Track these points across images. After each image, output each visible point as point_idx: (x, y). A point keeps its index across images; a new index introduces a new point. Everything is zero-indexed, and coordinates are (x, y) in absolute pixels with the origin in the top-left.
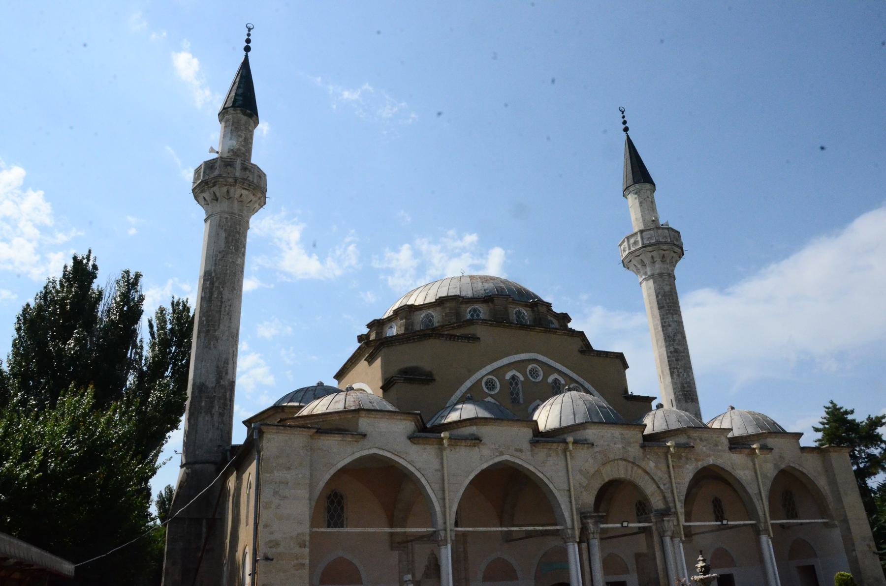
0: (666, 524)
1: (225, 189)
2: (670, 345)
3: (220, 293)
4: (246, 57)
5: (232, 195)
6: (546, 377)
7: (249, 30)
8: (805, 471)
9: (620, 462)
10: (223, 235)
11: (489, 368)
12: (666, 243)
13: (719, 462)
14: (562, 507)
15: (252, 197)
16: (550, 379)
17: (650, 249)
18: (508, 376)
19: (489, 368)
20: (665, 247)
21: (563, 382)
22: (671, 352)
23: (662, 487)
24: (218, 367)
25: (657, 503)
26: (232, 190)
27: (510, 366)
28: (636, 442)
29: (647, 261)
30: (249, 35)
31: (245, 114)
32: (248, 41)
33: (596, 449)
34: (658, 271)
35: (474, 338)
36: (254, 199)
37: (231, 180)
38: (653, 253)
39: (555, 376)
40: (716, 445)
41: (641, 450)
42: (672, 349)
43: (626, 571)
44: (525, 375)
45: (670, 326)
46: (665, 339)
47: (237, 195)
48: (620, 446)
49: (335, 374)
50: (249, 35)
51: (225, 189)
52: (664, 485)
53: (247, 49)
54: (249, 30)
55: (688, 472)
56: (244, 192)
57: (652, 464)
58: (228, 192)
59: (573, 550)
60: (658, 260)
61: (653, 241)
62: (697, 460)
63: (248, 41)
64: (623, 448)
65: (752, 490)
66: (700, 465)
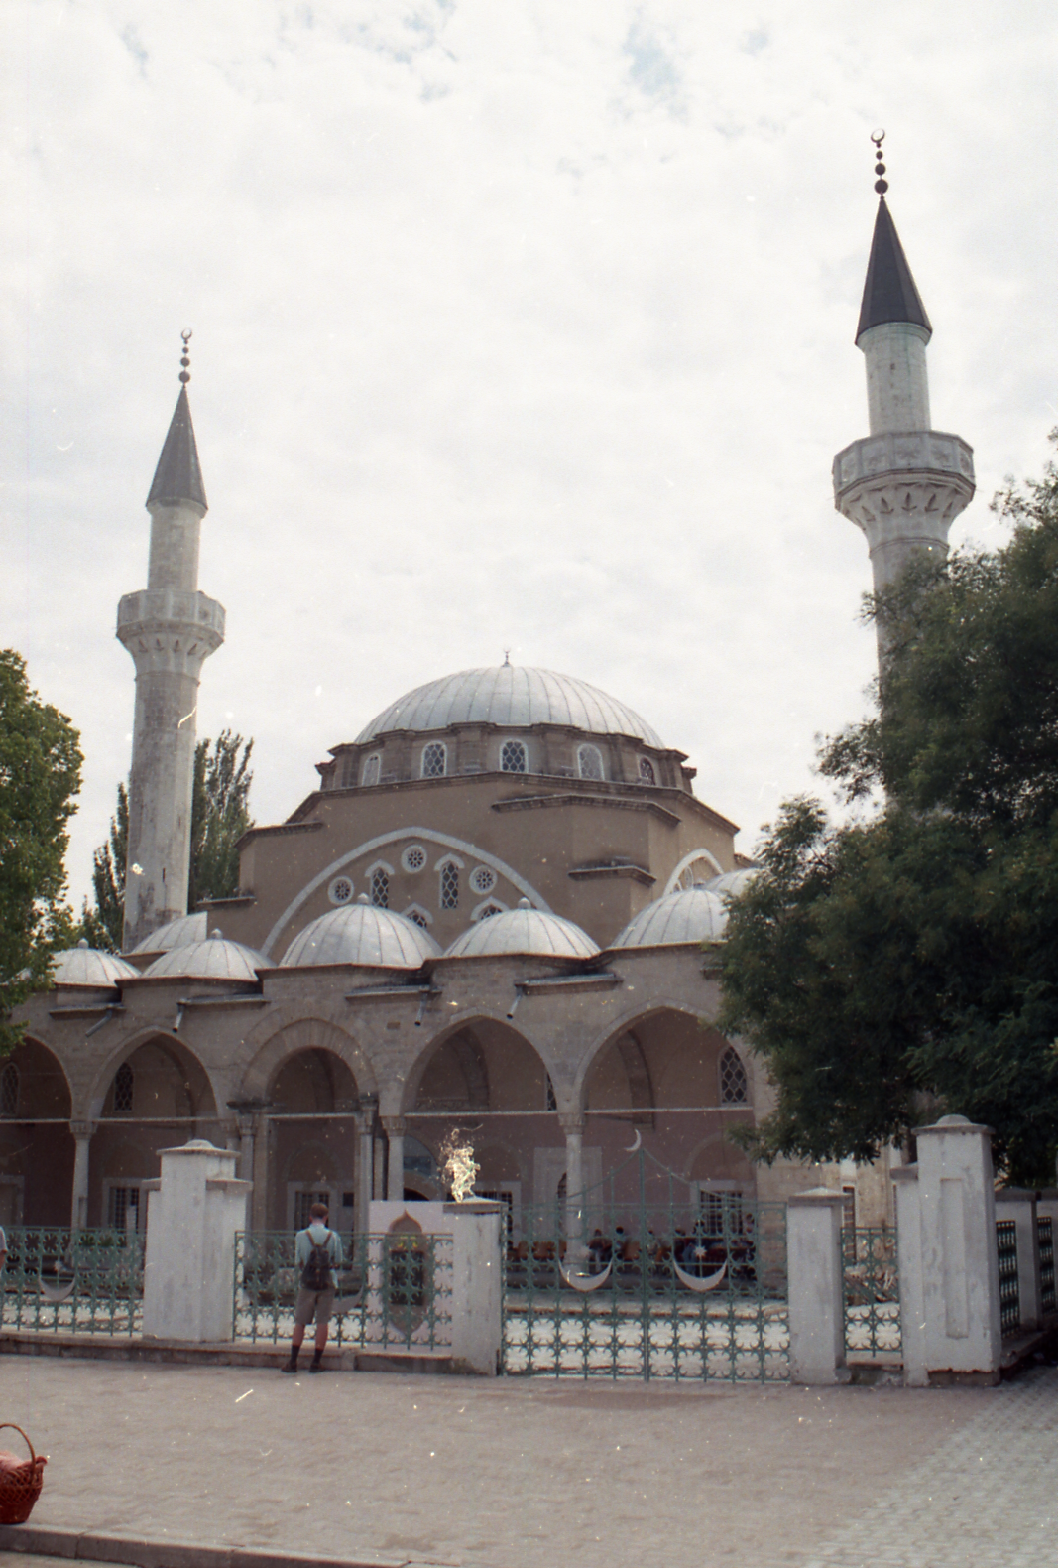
3: (140, 794)
6: (431, 864)
10: (143, 706)
11: (336, 866)
12: (874, 477)
15: (174, 638)
16: (439, 867)
18: (369, 873)
19: (336, 866)
21: (460, 864)
24: (140, 896)
25: (364, 1086)
26: (144, 642)
30: (186, 351)
32: (185, 362)
33: (274, 1007)
35: (318, 826)
50: (186, 351)
51: (135, 640)
53: (184, 377)
56: (161, 637)
58: (140, 643)
61: (853, 478)
63: (185, 362)
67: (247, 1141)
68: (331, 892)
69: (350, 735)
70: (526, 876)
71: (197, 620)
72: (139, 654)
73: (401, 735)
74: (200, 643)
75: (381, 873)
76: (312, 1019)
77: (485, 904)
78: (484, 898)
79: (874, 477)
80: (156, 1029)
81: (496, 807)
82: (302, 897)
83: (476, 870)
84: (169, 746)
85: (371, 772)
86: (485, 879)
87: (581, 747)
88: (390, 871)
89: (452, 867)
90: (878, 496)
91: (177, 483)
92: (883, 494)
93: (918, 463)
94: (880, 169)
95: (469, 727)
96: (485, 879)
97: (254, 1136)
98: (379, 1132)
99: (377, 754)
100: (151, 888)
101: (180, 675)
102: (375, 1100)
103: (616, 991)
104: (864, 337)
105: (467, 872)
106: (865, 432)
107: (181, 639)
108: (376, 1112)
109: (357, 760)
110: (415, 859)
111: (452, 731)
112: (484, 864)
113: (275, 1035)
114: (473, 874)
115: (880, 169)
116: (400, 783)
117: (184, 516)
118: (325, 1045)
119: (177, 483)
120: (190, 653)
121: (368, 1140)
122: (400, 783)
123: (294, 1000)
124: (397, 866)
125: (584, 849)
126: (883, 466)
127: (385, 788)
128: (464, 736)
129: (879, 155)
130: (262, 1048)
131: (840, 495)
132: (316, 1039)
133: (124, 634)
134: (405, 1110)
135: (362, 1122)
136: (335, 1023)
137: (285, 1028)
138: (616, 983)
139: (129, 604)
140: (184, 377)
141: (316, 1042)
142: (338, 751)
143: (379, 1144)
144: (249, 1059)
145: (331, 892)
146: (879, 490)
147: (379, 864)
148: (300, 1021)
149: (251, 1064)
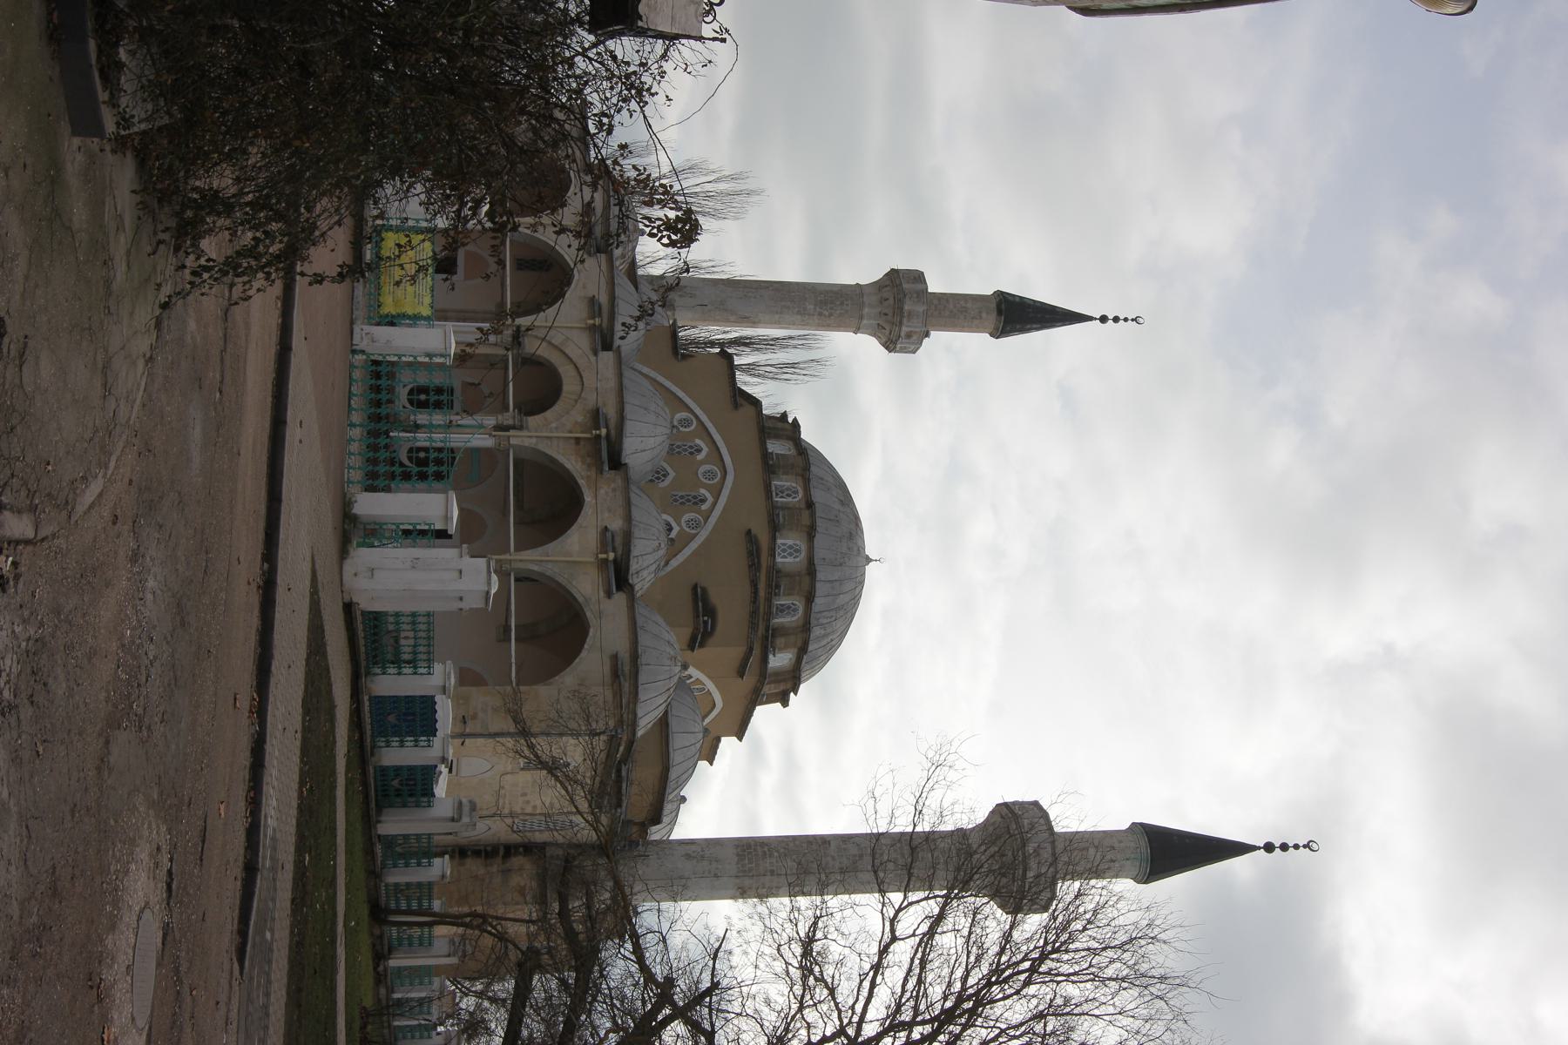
4: (1090, 318)
8: (584, 654)
11: (704, 418)
16: (703, 491)
18: (698, 441)
21: (704, 507)
25: (532, 421)
27: (714, 442)
30: (1126, 320)
32: (1116, 319)
33: (593, 359)
35: (736, 406)
39: (710, 499)
44: (702, 462)
47: (885, 295)
50: (1126, 320)
53: (1104, 319)
55: (573, 464)
56: (891, 301)
57: (580, 419)
63: (1116, 319)
66: (581, 482)
68: (684, 415)
69: (805, 435)
70: (696, 553)
71: (905, 329)
72: (879, 285)
73: (807, 468)
75: (699, 451)
77: (674, 524)
78: (679, 524)
81: (749, 532)
82: (681, 394)
85: (775, 447)
86: (695, 524)
87: (800, 606)
88: (700, 457)
89: (703, 501)
91: (1015, 315)
94: (1284, 847)
95: (813, 516)
96: (695, 524)
99: (793, 452)
100: (692, 296)
101: (861, 318)
106: (1057, 829)
108: (513, 427)
109: (789, 438)
110: (710, 475)
115: (1284, 847)
116: (770, 466)
117: (991, 319)
119: (1015, 315)
122: (770, 466)
124: (702, 462)
125: (715, 598)
127: (766, 455)
128: (806, 514)
129: (1296, 847)
131: (1006, 804)
132: (569, 385)
133: (894, 274)
134: (513, 446)
135: (508, 418)
138: (609, 595)
139: (918, 277)
140: (1104, 319)
141: (565, 388)
142: (796, 424)
145: (684, 415)
147: (705, 450)
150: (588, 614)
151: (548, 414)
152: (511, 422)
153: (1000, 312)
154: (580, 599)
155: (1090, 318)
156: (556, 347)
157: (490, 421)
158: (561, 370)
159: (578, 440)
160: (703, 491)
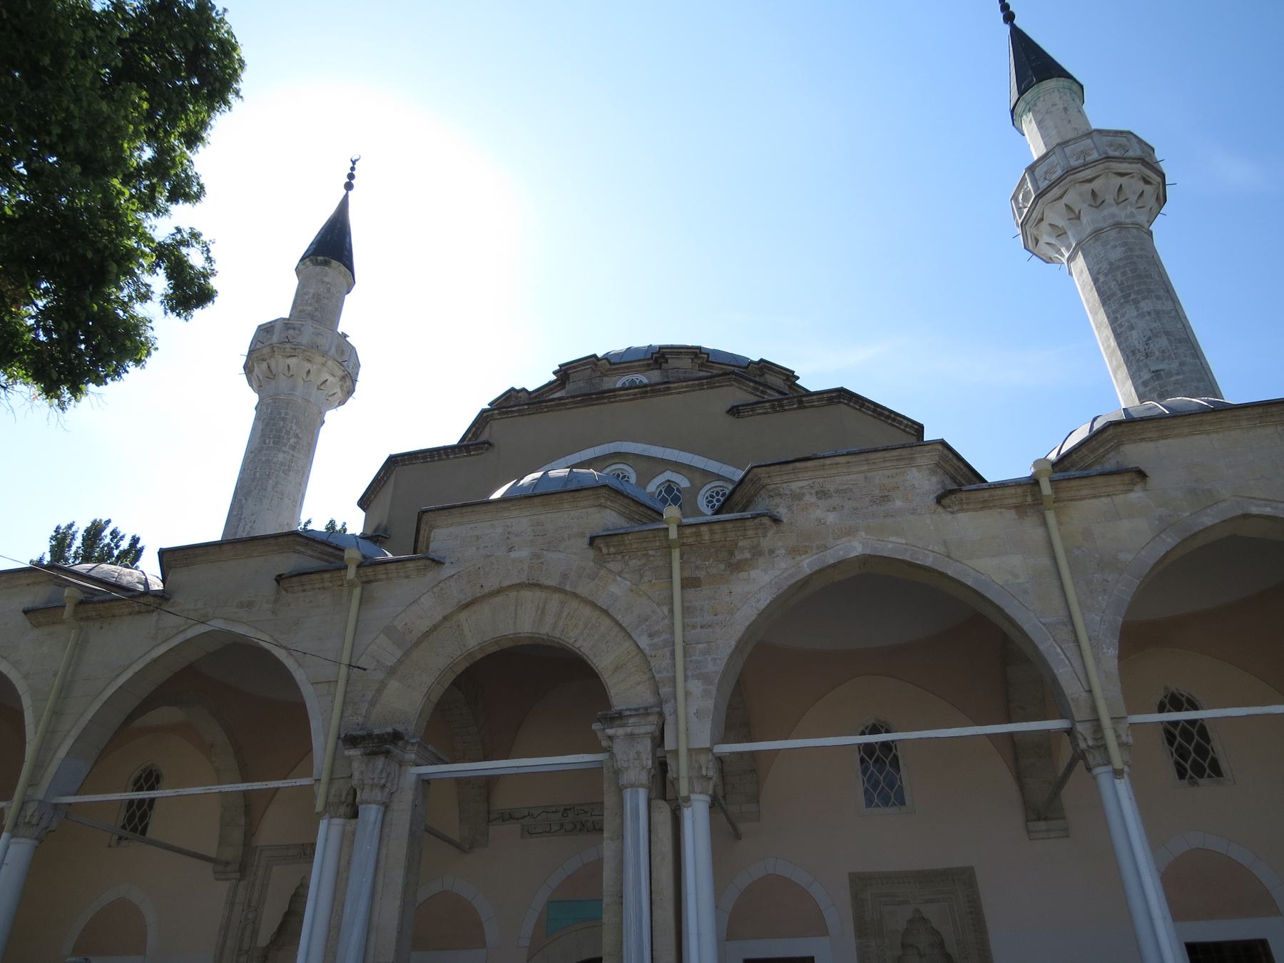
0: (618, 748)
1: (264, 365)
2: (1139, 370)
3: (241, 507)
4: (346, 197)
5: (273, 368)
7: (354, 163)
9: (527, 594)
12: (1085, 166)
13: (891, 545)
14: (315, 725)
15: (308, 366)
16: (652, 487)
17: (1056, 192)
20: (1088, 174)
21: (683, 482)
22: (1145, 384)
23: (644, 642)
25: (625, 690)
28: (582, 535)
29: (1061, 223)
30: (353, 169)
31: (317, 263)
32: (351, 176)
33: (447, 571)
34: (1089, 230)
36: (313, 368)
37: (266, 350)
38: (1065, 200)
39: (668, 475)
40: (885, 499)
41: (591, 553)
42: (1146, 376)
43: (819, 928)
45: (1132, 328)
46: (1128, 362)
48: (523, 553)
49: (144, 553)
50: (353, 169)
51: (264, 365)
52: (651, 636)
53: (349, 186)
54: (354, 163)
56: (292, 361)
59: (328, 833)
60: (1082, 207)
62: (794, 551)
63: (351, 176)
64: (535, 556)
65: (1032, 617)
66: (807, 564)
67: (370, 813)
74: (331, 379)
76: (520, 586)
79: (1085, 166)
80: (219, 624)
81: (734, 411)
83: (708, 486)
84: (282, 464)
90: (1089, 186)
91: (332, 248)
92: (1095, 185)
93: (1131, 154)
97: (386, 807)
98: (662, 782)
102: (657, 712)
103: (1137, 495)
104: (1028, 95)
105: (694, 490)
107: (313, 368)
108: (659, 740)
111: (656, 361)
112: (719, 477)
113: (445, 618)
114: (703, 492)
118: (545, 630)
119: (332, 248)
120: (318, 389)
121: (642, 795)
123: (488, 556)
126: (1095, 156)
128: (673, 362)
130: (418, 643)
132: (524, 620)
134: (715, 742)
136: (568, 588)
137: (468, 605)
140: (349, 186)
143: (663, 815)
144: (390, 662)
146: (1090, 181)
148: (500, 591)
149: (392, 671)
150: (1208, 520)
151: (603, 662)
152: (646, 746)
153: (326, 263)
154: (1170, 541)
155: (346, 197)
156: (407, 654)
157: (637, 800)
158: (472, 642)
159: (690, 583)
160: (652, 487)
